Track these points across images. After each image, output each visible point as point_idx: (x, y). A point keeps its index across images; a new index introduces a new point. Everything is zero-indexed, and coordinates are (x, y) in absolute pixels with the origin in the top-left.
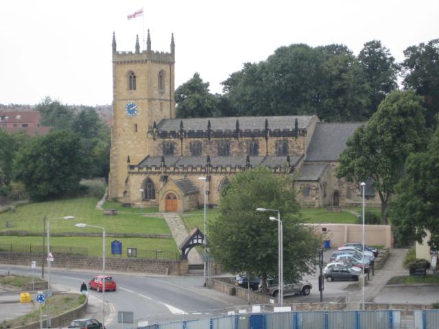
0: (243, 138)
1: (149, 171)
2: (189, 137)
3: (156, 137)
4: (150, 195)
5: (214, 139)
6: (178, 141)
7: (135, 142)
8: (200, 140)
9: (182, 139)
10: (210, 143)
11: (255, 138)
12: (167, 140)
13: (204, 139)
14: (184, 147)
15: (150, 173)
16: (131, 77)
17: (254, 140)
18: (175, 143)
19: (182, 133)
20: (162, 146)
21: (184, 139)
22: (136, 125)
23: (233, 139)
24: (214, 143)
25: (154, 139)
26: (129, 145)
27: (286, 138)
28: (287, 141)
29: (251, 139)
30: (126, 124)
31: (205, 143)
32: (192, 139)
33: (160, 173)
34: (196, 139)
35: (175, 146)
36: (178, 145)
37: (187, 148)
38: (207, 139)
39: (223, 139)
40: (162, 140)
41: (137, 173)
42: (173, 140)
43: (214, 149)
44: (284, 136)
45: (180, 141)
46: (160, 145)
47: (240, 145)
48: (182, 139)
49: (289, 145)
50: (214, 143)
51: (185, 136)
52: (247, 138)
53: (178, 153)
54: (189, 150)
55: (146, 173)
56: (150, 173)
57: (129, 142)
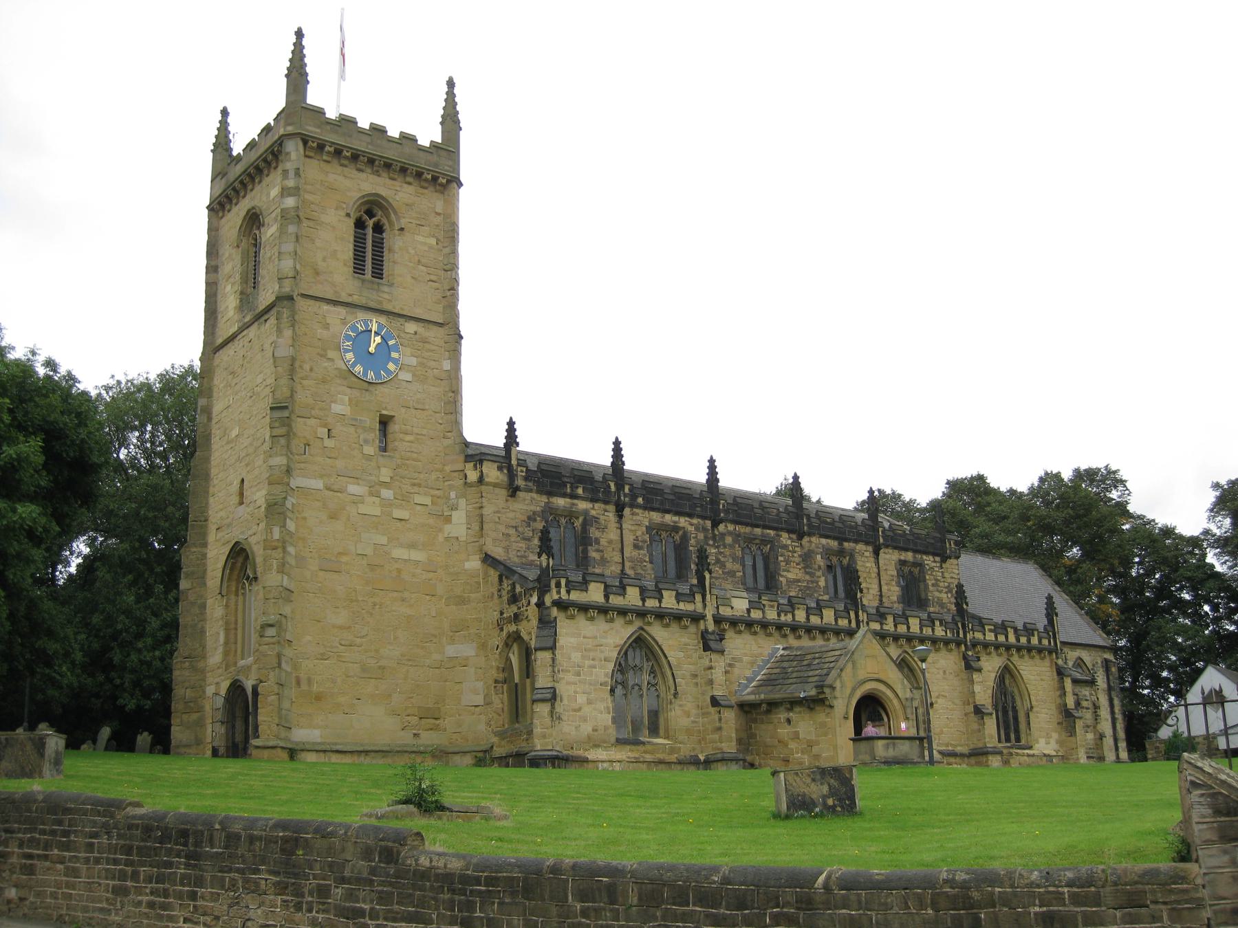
2: (647, 507)
5: (731, 527)
6: (608, 515)
7: (387, 494)
8: (683, 522)
11: (846, 544)
12: (561, 502)
13: (695, 521)
14: (629, 539)
15: (660, 615)
16: (360, 224)
18: (588, 521)
19: (620, 487)
21: (627, 511)
22: (384, 422)
23: (785, 538)
24: (729, 540)
25: (513, 491)
26: (358, 500)
28: (920, 565)
29: (834, 544)
31: (701, 536)
32: (656, 517)
33: (696, 618)
34: (669, 518)
35: (594, 533)
36: (603, 529)
37: (636, 547)
38: (708, 523)
39: (758, 531)
40: (544, 499)
41: (603, 610)
42: (582, 505)
44: (915, 551)
45: (611, 516)
46: (531, 518)
47: (807, 558)
50: (729, 540)
51: (634, 497)
52: (824, 541)
53: (604, 562)
55: (642, 614)
56: (660, 615)
57: (353, 489)
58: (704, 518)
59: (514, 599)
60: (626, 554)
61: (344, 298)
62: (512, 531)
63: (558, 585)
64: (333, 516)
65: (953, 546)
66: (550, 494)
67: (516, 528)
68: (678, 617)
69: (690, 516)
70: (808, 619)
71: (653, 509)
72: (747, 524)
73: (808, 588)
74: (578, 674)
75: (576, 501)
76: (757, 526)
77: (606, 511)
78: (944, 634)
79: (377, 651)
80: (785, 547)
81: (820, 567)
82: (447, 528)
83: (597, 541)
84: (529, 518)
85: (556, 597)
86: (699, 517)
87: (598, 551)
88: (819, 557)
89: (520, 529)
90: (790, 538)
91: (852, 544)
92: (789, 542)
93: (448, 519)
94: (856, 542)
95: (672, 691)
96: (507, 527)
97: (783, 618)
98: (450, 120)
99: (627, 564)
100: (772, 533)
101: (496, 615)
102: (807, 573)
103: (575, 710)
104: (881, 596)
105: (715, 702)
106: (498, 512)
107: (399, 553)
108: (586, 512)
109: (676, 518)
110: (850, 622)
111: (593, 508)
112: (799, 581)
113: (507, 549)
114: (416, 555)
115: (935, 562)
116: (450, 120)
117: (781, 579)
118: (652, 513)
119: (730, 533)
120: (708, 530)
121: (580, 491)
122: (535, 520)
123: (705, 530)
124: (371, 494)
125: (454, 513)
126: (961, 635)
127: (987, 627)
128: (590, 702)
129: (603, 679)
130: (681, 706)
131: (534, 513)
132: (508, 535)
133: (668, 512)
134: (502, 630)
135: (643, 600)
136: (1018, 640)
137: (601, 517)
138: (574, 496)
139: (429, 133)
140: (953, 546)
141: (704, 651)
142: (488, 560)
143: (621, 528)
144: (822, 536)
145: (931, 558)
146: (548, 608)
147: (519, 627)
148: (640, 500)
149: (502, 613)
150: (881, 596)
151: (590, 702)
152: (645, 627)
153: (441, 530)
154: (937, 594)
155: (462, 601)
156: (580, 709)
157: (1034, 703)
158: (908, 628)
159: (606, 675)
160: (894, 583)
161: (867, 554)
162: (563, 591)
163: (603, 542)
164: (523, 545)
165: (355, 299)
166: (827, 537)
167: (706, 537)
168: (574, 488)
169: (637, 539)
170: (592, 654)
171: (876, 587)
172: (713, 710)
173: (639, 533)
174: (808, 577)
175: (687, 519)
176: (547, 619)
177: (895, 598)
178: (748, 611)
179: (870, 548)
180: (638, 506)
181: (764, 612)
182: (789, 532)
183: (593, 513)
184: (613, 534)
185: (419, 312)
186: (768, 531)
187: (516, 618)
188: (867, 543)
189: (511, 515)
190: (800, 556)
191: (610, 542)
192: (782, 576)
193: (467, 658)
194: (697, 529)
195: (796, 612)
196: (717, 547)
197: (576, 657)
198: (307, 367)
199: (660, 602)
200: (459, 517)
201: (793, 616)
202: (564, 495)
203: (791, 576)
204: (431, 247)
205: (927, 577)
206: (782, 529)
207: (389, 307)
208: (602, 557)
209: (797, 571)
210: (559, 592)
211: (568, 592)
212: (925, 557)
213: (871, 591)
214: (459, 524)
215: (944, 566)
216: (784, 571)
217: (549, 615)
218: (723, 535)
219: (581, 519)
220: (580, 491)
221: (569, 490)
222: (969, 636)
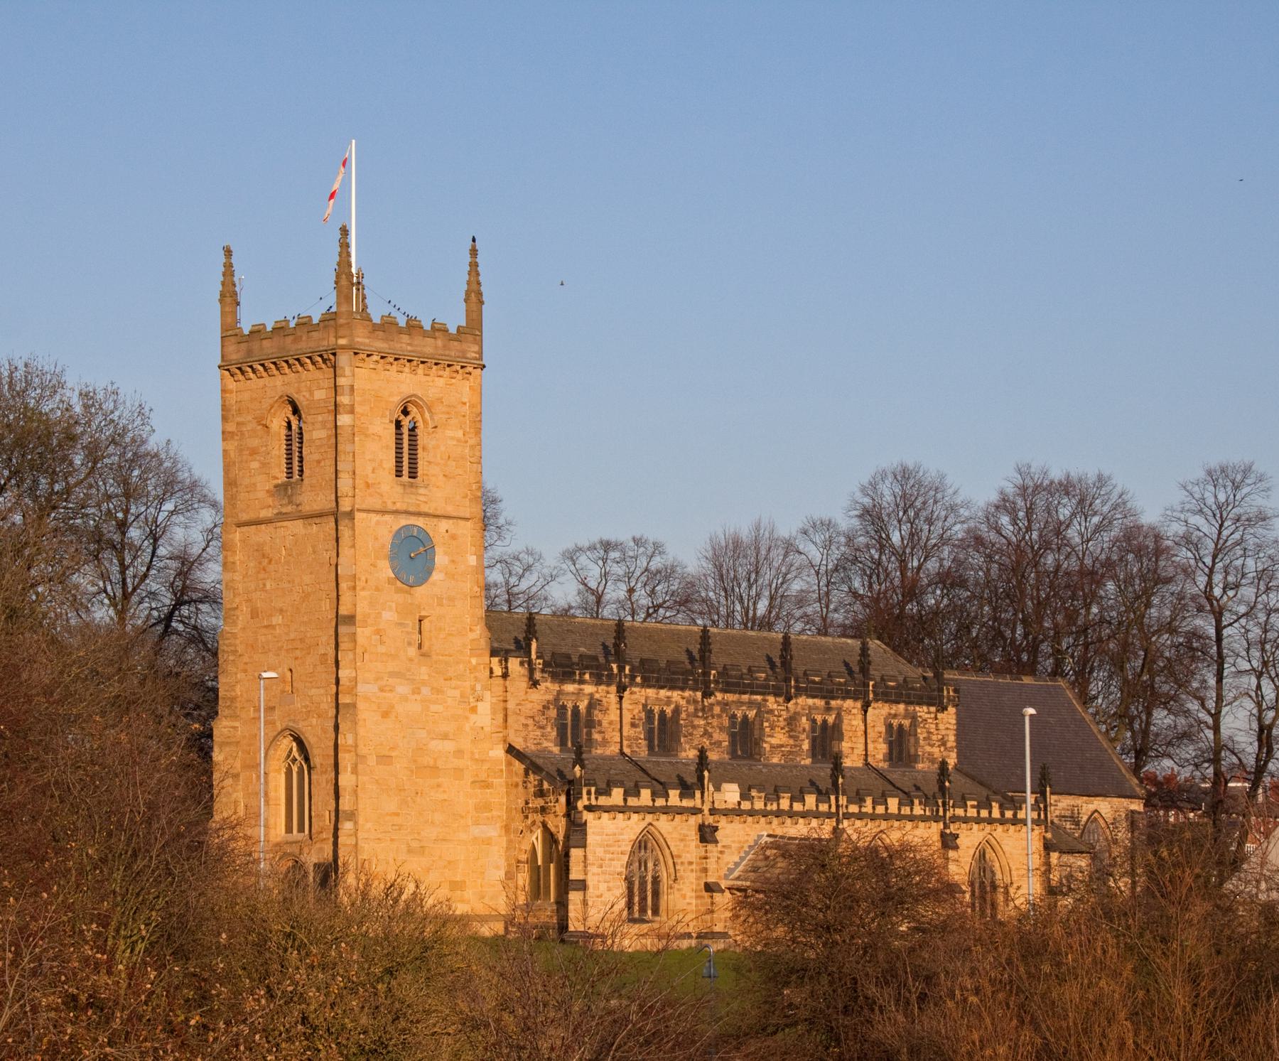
0: (802, 700)
1: (660, 802)
2: (646, 683)
3: (538, 675)
4: (643, 899)
8: (676, 695)
9: (621, 689)
10: (706, 711)
11: (833, 703)
12: (570, 688)
13: (687, 694)
14: (627, 718)
15: (666, 810)
17: (828, 709)
18: (593, 704)
20: (553, 713)
24: (717, 710)
25: (535, 684)
26: (404, 699)
27: (911, 708)
28: (914, 718)
29: (820, 703)
30: (388, 616)
31: (691, 709)
32: (651, 692)
35: (597, 715)
36: (605, 711)
37: (633, 725)
38: (699, 694)
39: (745, 697)
40: (556, 687)
42: (589, 689)
43: (717, 736)
44: (908, 703)
45: (613, 698)
48: (621, 689)
49: (921, 733)
50: (717, 710)
52: (810, 701)
53: (605, 743)
54: (640, 732)
57: (403, 689)
58: (695, 690)
59: (540, 793)
60: (625, 734)
61: (390, 507)
62: (530, 722)
63: (589, 793)
64: (385, 715)
65: (951, 693)
66: (562, 682)
67: (532, 717)
68: (680, 811)
69: (683, 689)
70: (791, 806)
71: (649, 687)
72: (735, 692)
73: (790, 753)
74: (601, 867)
75: (582, 686)
76: (744, 693)
77: (608, 692)
78: (922, 812)
79: (419, 833)
80: (771, 712)
81: (804, 730)
82: (473, 717)
83: (600, 723)
84: (544, 707)
85: (587, 803)
86: (690, 690)
87: (600, 732)
88: (804, 719)
89: (537, 719)
90: (776, 702)
91: (839, 702)
92: (775, 706)
93: (474, 710)
94: (844, 699)
95: (673, 878)
96: (527, 717)
97: (769, 808)
98: (474, 296)
99: (625, 743)
100: (759, 698)
101: (521, 803)
102: (790, 737)
103: (598, 897)
104: (866, 755)
105: (709, 888)
106: (518, 705)
107: (436, 745)
108: (591, 695)
109: (669, 693)
110: (830, 807)
111: (597, 692)
112: (782, 746)
113: (525, 740)
114: (449, 746)
115: (929, 713)
116: (474, 296)
117: (765, 745)
118: (648, 690)
119: (718, 703)
120: (698, 702)
121: (587, 677)
122: (549, 708)
123: (695, 702)
124: (414, 693)
125: (479, 704)
126: (941, 813)
127: (969, 803)
128: (609, 889)
129: (619, 870)
130: (678, 890)
131: (548, 702)
132: (527, 725)
133: (662, 687)
134: (527, 817)
135: (654, 801)
136: (1002, 814)
137: (604, 700)
138: (582, 682)
139: (455, 318)
140: (951, 693)
141: (701, 842)
142: (511, 750)
143: (621, 709)
144: (809, 696)
145: (925, 708)
146: (581, 812)
147: (546, 819)
148: (638, 680)
149: (527, 803)
150: (866, 755)
151: (609, 889)
152: (654, 823)
153: (467, 718)
154: (928, 749)
155: (486, 785)
156: (601, 896)
157: (1015, 879)
158: (887, 809)
159: (622, 866)
160: (881, 740)
161: (855, 711)
162: (593, 796)
163: (605, 723)
164: (538, 733)
165: (399, 506)
166: (814, 697)
167: (696, 710)
168: (582, 674)
169: (633, 718)
170: (611, 849)
171: (862, 747)
172: (706, 894)
173: (636, 712)
174: (791, 742)
175: (680, 692)
176: (579, 821)
177: (880, 757)
178: (739, 803)
179: (859, 704)
180: (637, 685)
181: (752, 804)
182: (776, 695)
183: (597, 696)
184: (614, 715)
185: (450, 510)
186: (755, 697)
187: (543, 810)
188: (856, 699)
189: (529, 706)
190: (785, 720)
191: (611, 723)
192: (766, 742)
193: (490, 838)
194: (688, 702)
195: (781, 801)
196: (706, 718)
197: (600, 852)
198: (363, 578)
199: (667, 801)
200: (484, 708)
201: (778, 805)
202: (574, 682)
203: (774, 741)
204: (459, 440)
205: (919, 731)
206: (769, 694)
207: (425, 509)
208: (604, 738)
209: (781, 736)
210: (589, 799)
211: (597, 798)
212: (917, 708)
213: (855, 751)
214: (485, 715)
215: (939, 716)
216: (769, 736)
217: (581, 818)
218: (712, 705)
219: (586, 702)
220: (587, 677)
221: (577, 678)
222: (948, 815)
